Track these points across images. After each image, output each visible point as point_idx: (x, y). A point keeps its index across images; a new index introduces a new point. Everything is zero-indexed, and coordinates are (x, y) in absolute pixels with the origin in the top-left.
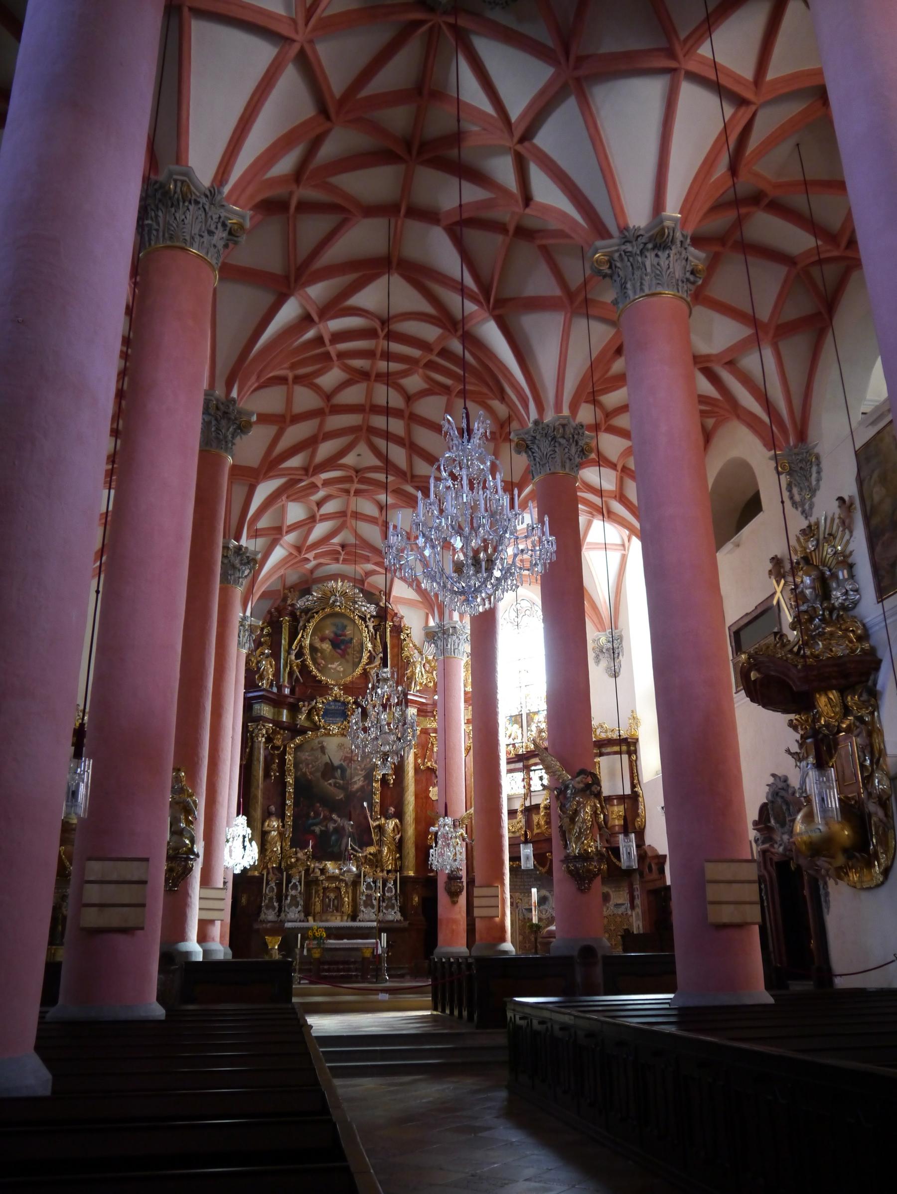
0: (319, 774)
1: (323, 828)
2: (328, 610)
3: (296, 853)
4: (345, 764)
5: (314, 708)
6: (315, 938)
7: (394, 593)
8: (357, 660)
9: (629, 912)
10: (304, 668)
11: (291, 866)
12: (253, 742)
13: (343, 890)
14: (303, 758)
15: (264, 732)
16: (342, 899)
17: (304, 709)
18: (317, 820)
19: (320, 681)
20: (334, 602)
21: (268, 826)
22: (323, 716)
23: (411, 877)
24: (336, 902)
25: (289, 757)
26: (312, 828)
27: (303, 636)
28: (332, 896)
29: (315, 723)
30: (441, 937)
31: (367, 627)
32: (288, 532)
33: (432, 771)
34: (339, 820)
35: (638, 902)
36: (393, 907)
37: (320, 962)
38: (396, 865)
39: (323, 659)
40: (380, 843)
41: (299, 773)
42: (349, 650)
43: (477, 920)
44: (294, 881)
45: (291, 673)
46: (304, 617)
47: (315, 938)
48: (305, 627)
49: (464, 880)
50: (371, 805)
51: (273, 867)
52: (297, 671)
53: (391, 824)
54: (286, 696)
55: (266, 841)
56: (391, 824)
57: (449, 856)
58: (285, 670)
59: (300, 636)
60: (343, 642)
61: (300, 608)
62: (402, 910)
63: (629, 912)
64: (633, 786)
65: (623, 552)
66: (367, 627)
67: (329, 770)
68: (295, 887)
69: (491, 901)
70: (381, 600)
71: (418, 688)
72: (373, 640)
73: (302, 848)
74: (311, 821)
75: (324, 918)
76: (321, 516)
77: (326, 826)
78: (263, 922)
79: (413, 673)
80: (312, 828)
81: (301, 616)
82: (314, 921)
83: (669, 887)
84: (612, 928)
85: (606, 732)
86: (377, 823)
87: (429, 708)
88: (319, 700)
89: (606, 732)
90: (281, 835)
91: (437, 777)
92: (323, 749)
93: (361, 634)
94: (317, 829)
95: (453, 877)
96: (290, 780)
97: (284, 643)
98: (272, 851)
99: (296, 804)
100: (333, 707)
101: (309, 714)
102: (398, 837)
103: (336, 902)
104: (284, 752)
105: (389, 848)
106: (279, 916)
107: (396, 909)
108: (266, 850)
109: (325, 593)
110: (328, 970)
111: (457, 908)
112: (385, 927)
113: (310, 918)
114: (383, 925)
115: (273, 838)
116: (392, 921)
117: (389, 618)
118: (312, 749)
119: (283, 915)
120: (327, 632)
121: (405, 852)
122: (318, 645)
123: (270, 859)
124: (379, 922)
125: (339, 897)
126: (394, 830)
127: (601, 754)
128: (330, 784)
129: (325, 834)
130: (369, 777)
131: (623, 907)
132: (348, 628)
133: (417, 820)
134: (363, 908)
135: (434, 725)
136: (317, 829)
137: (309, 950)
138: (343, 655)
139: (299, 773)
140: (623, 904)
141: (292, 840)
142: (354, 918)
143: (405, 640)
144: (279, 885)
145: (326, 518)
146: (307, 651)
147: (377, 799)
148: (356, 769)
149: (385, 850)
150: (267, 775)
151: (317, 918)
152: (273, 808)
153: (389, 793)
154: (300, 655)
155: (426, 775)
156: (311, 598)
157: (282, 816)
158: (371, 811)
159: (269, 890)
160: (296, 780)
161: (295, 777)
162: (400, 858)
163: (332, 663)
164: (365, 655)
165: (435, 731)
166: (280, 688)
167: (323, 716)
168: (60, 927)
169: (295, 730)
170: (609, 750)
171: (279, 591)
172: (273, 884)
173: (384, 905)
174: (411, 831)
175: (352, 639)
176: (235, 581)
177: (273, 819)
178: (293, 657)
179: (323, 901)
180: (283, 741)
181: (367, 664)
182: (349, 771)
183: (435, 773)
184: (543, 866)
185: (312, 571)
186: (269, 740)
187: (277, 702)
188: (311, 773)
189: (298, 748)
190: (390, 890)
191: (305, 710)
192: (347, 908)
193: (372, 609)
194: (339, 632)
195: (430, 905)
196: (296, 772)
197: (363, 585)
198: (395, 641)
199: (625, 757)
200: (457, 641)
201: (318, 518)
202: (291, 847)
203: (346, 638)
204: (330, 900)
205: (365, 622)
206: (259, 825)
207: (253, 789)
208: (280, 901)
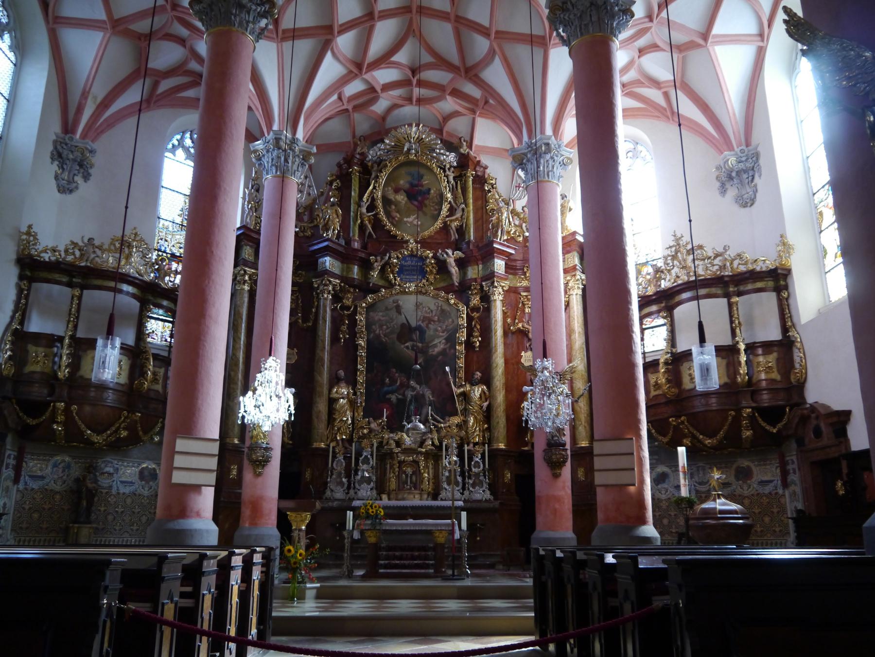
0: (395, 336)
1: (400, 397)
2: (402, 158)
3: (369, 423)
4: (423, 325)
5: (387, 264)
6: (368, 516)
7: (477, 142)
8: (436, 212)
9: (780, 491)
10: (377, 223)
11: (364, 436)
12: (319, 300)
13: (422, 464)
14: (376, 318)
15: (330, 288)
16: (421, 474)
17: (376, 264)
18: (394, 387)
19: (395, 236)
20: (409, 150)
21: (337, 392)
22: (399, 273)
23: (501, 450)
24: (414, 478)
25: (361, 318)
26: (387, 396)
27: (374, 188)
28: (409, 471)
29: (390, 282)
30: (540, 520)
31: (447, 176)
32: (341, 32)
33: (523, 333)
34: (418, 387)
35: (794, 477)
36: (481, 484)
37: (376, 547)
38: (484, 437)
39: (398, 212)
40: (466, 412)
41: (372, 335)
42: (427, 202)
43: (599, 491)
44: (365, 454)
45: (362, 227)
46: (375, 168)
47: (368, 516)
48: (377, 177)
49: (568, 447)
50: (454, 371)
51: (342, 439)
52: (369, 226)
53: (477, 392)
54: (357, 250)
55: (335, 409)
56: (477, 392)
57: (552, 410)
58: (355, 223)
59: (371, 188)
60: (420, 193)
61: (371, 160)
62: (492, 488)
63: (780, 491)
64: (785, 330)
65: (761, 44)
66: (447, 176)
67: (406, 331)
68: (366, 461)
69: (623, 462)
70: (461, 146)
71: (506, 238)
72: (453, 191)
73: (375, 419)
74: (386, 389)
75: (400, 496)
76: (380, 12)
77: (404, 395)
78: (328, 500)
79: (499, 220)
80: (387, 396)
81: (372, 167)
82: (389, 499)
83: (865, 453)
84: (757, 511)
85: (746, 264)
86: (462, 390)
87: (519, 264)
88: (394, 254)
89: (746, 264)
90: (352, 404)
91: (530, 340)
92: (398, 309)
93: (439, 182)
94: (393, 398)
95: (553, 444)
96: (362, 342)
97: (354, 194)
98: (342, 420)
99: (369, 370)
100: (409, 263)
101: (383, 270)
102: (486, 404)
103: (414, 478)
104: (355, 312)
105: (475, 418)
106: (348, 493)
107: (485, 485)
108: (335, 419)
109: (399, 140)
110: (400, 558)
111: (560, 482)
112: (473, 510)
113: (384, 497)
114: (469, 505)
115: (343, 406)
116: (480, 501)
117: (471, 166)
118: (387, 309)
119: (352, 492)
120: (402, 182)
121: (494, 422)
122: (392, 196)
123: (339, 429)
124: (465, 501)
125: (417, 473)
126: (481, 397)
127: (740, 294)
128: (407, 347)
129: (402, 402)
130: (451, 340)
131: (772, 484)
132: (425, 177)
133: (508, 388)
134: (445, 485)
135: (525, 283)
136: (393, 398)
137: (362, 533)
138: (420, 207)
139: (372, 335)
140: (771, 481)
141: (365, 410)
142: (435, 496)
143: (489, 191)
144: (348, 459)
145: (387, 14)
146: (379, 203)
147: (461, 363)
148: (436, 330)
149: (472, 420)
150: (335, 339)
151: (392, 496)
152: (342, 373)
153: (475, 358)
154: (372, 207)
155: (518, 338)
156: (383, 147)
157: (352, 382)
158: (454, 377)
159: (339, 464)
160: (369, 342)
161: (367, 340)
162: (489, 429)
163: (408, 216)
164: (445, 208)
165: (527, 289)
166: (348, 242)
167: (399, 273)
168: (84, 503)
169: (366, 288)
170: (750, 287)
171: (349, 142)
172: (341, 458)
173: (471, 482)
174: (500, 397)
175: (429, 190)
176: (241, 24)
177: (343, 384)
178: (364, 210)
179: (398, 477)
180: (353, 302)
181: (447, 216)
182: (428, 333)
183: (527, 336)
184: (664, 436)
185: (384, 118)
186: (337, 298)
187: (345, 256)
188: (385, 336)
189: (371, 307)
190: (477, 465)
191: (377, 266)
192: (427, 486)
193: (451, 158)
194: (416, 182)
195: (525, 484)
196: (368, 335)
197: (442, 134)
198: (479, 193)
199: (773, 296)
200: (551, 162)
201: (376, 15)
202: (364, 417)
203: (424, 189)
204: (407, 476)
205: (445, 171)
206: (325, 391)
207: (318, 351)
208: (348, 476)
